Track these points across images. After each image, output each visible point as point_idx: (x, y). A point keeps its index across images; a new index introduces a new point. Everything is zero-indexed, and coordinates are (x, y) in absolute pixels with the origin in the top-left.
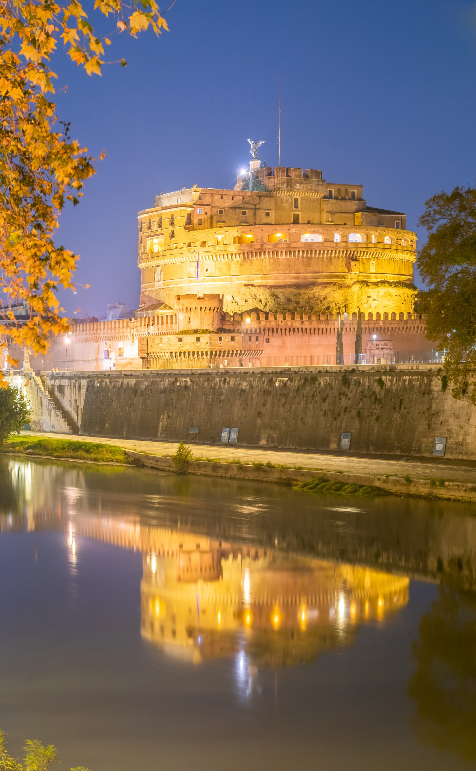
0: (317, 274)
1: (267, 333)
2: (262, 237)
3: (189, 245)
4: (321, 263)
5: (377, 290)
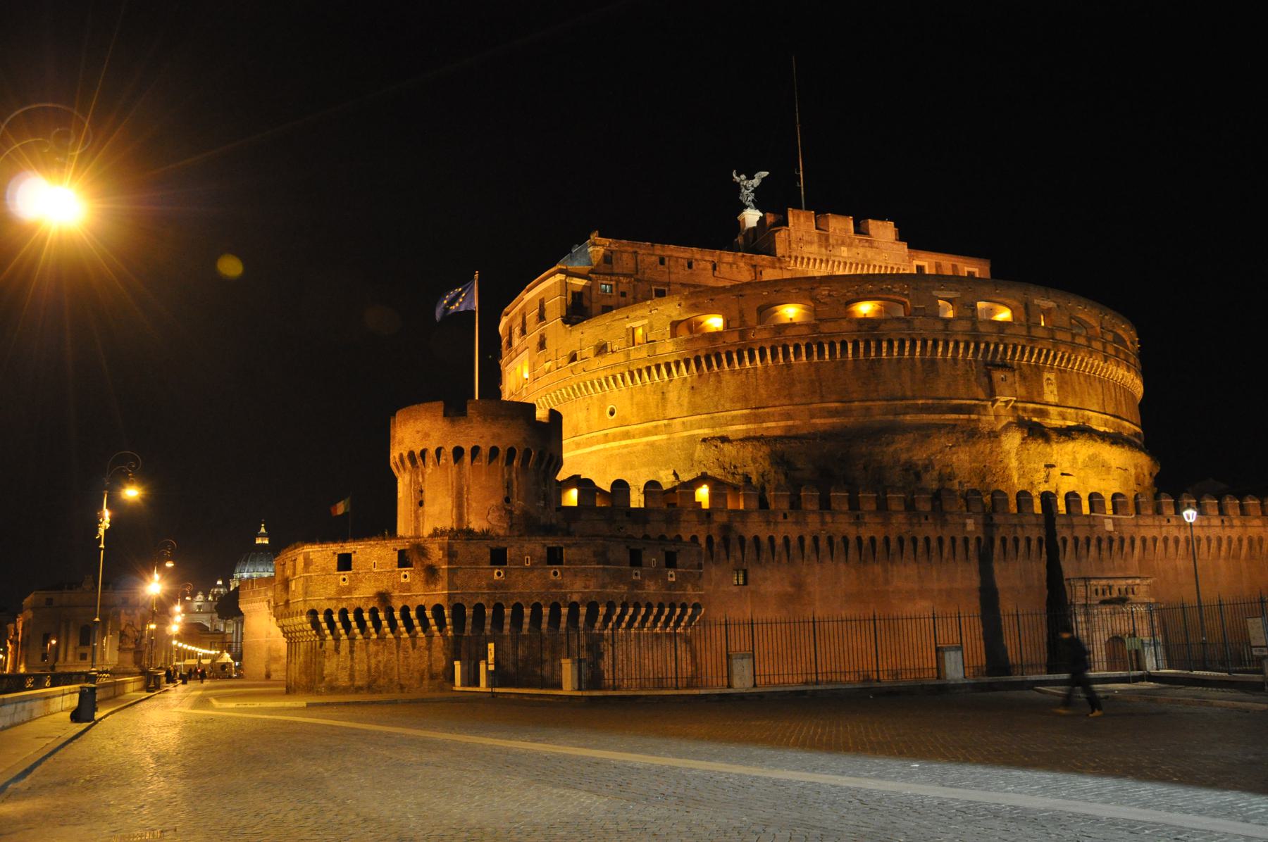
1: (739, 554)
2: (741, 312)
3: (573, 358)
5: (1070, 446)
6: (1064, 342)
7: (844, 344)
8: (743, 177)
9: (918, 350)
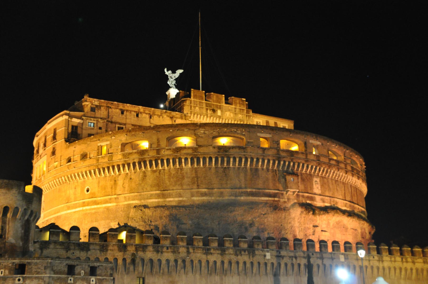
0: (237, 190)
1: (140, 269)
2: (158, 140)
3: (69, 160)
4: (242, 175)
6: (324, 163)
7: (211, 159)
8: (170, 72)
9: (249, 163)
